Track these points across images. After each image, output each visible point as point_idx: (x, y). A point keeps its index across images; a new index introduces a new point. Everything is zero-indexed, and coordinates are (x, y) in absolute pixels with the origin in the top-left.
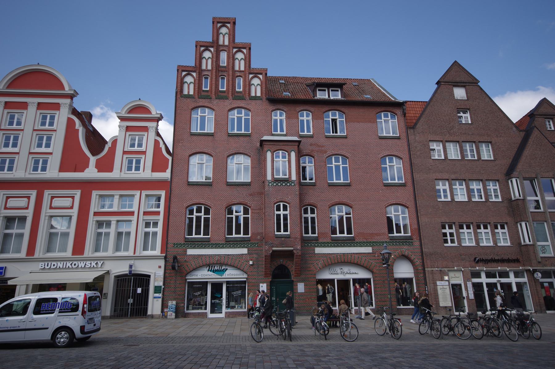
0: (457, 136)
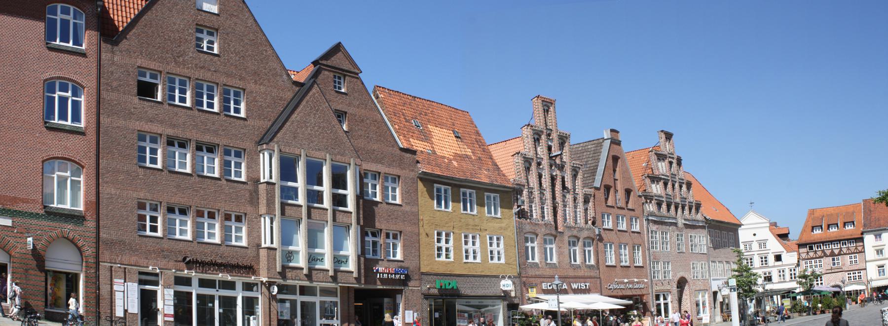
0: (188, 68)
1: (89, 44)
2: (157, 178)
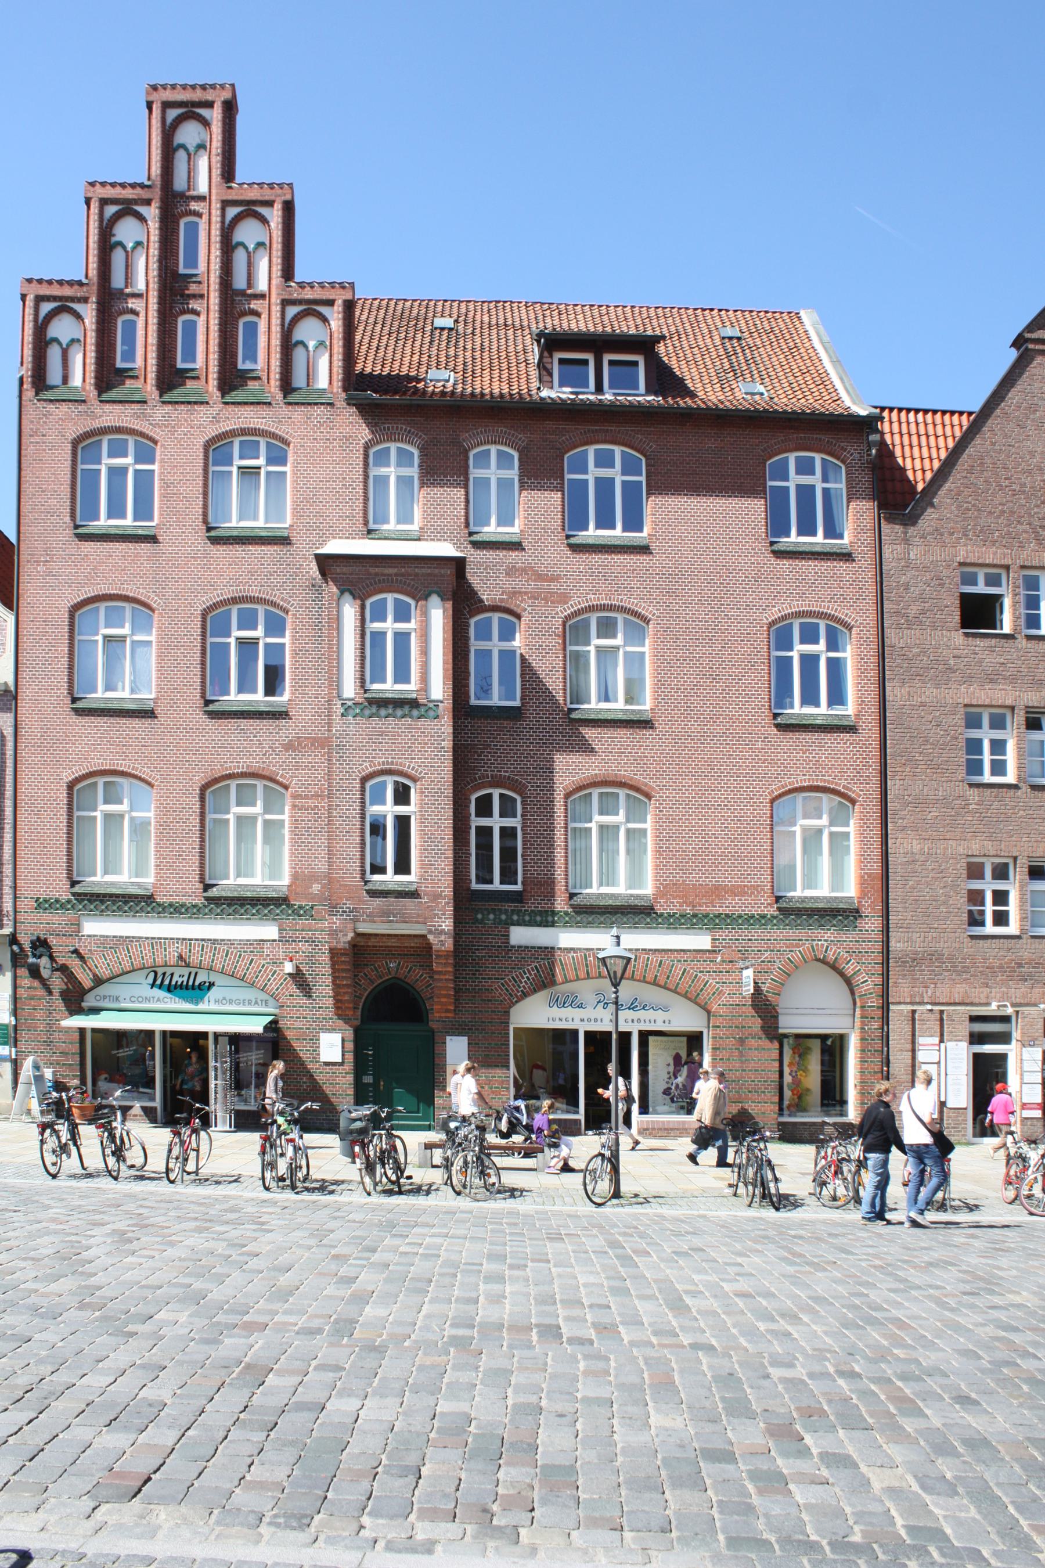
1: (858, 531)
2: (1006, 805)
